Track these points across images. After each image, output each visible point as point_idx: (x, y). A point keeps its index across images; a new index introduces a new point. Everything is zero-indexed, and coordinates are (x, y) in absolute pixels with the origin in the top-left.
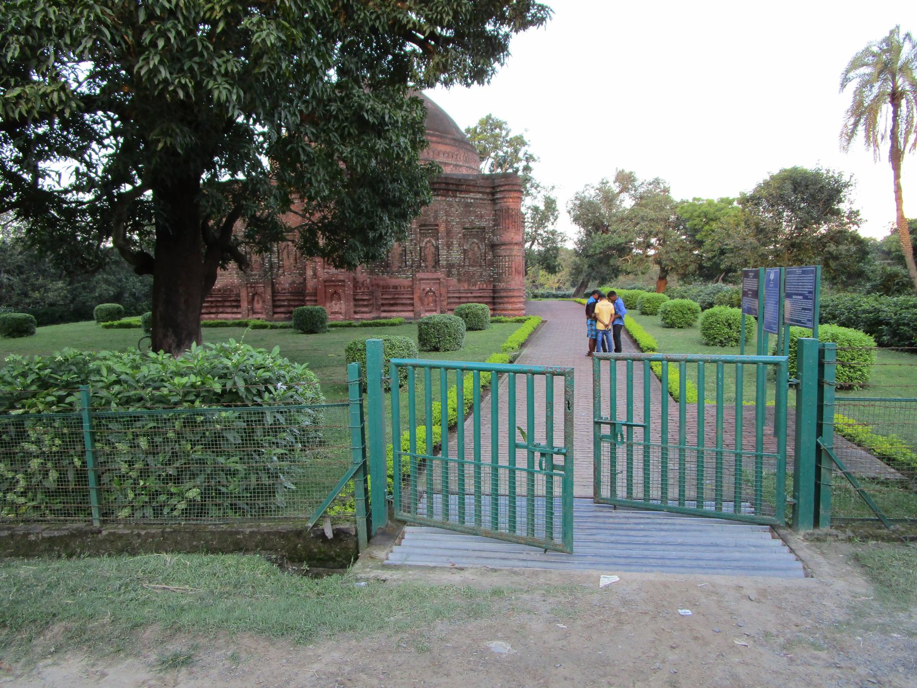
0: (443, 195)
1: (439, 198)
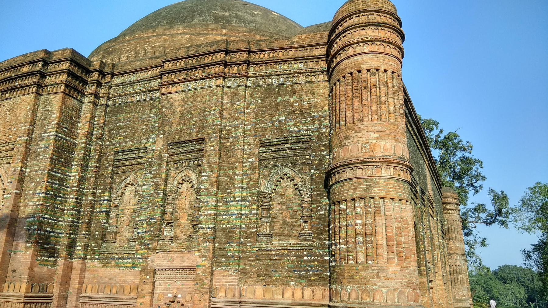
0: (217, 76)
1: (211, 82)
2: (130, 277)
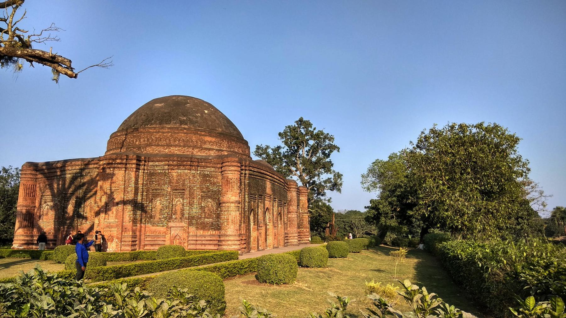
0: (188, 169)
1: (186, 171)
2: (163, 229)
